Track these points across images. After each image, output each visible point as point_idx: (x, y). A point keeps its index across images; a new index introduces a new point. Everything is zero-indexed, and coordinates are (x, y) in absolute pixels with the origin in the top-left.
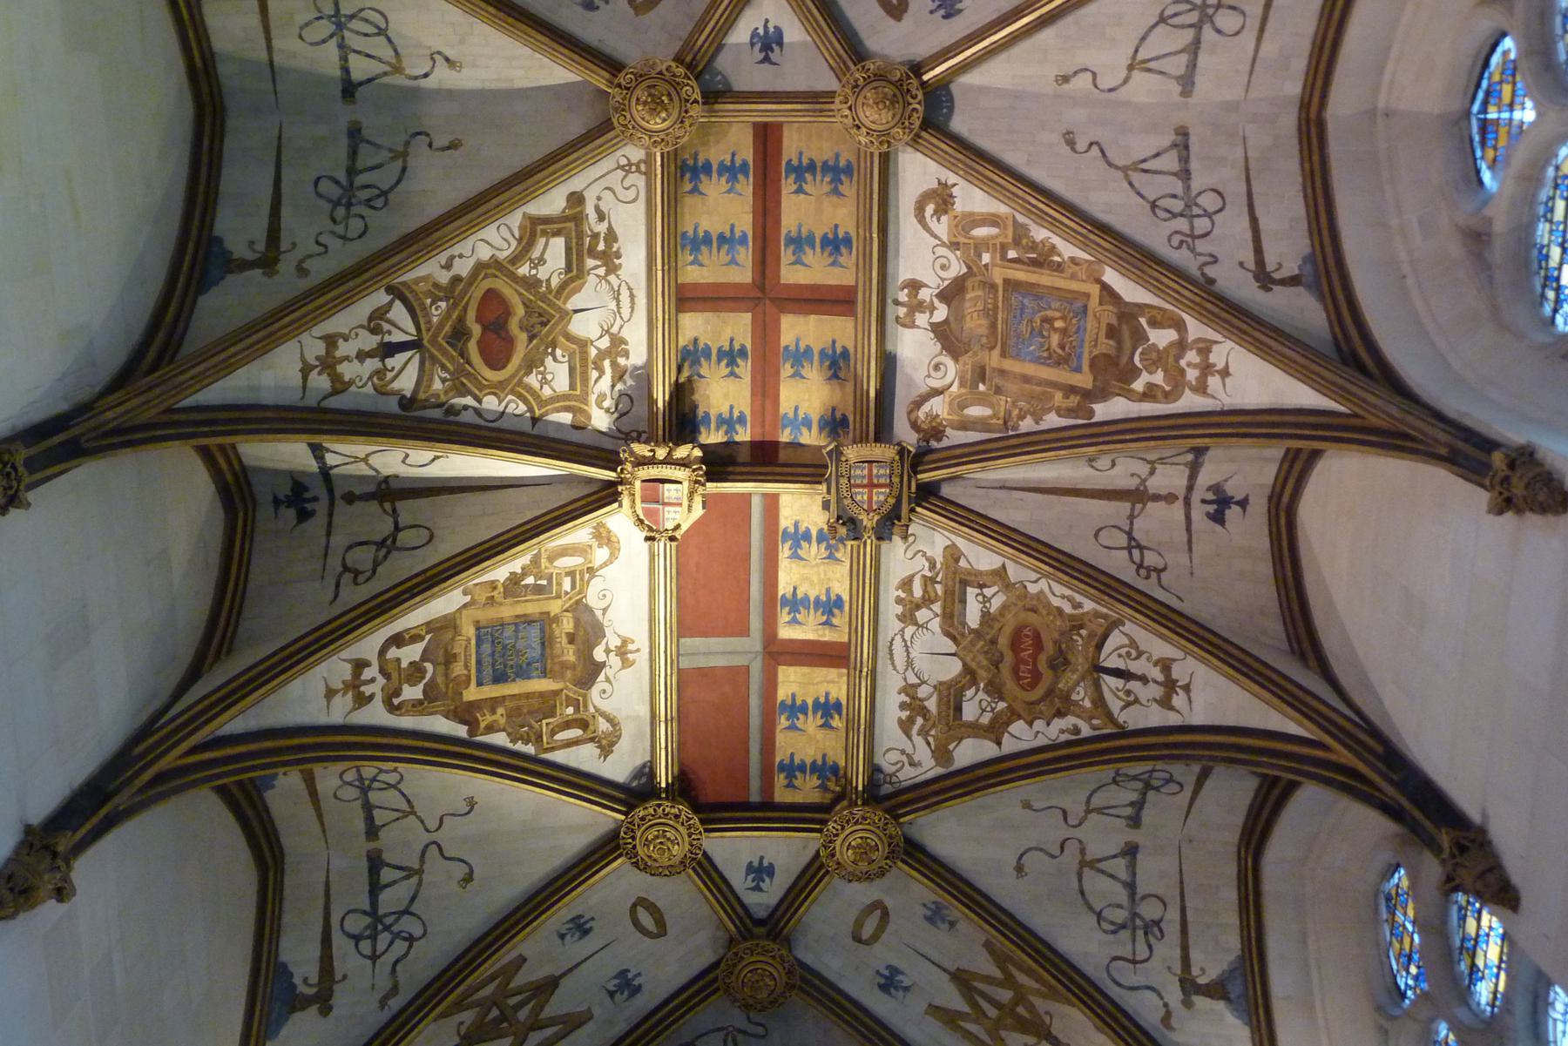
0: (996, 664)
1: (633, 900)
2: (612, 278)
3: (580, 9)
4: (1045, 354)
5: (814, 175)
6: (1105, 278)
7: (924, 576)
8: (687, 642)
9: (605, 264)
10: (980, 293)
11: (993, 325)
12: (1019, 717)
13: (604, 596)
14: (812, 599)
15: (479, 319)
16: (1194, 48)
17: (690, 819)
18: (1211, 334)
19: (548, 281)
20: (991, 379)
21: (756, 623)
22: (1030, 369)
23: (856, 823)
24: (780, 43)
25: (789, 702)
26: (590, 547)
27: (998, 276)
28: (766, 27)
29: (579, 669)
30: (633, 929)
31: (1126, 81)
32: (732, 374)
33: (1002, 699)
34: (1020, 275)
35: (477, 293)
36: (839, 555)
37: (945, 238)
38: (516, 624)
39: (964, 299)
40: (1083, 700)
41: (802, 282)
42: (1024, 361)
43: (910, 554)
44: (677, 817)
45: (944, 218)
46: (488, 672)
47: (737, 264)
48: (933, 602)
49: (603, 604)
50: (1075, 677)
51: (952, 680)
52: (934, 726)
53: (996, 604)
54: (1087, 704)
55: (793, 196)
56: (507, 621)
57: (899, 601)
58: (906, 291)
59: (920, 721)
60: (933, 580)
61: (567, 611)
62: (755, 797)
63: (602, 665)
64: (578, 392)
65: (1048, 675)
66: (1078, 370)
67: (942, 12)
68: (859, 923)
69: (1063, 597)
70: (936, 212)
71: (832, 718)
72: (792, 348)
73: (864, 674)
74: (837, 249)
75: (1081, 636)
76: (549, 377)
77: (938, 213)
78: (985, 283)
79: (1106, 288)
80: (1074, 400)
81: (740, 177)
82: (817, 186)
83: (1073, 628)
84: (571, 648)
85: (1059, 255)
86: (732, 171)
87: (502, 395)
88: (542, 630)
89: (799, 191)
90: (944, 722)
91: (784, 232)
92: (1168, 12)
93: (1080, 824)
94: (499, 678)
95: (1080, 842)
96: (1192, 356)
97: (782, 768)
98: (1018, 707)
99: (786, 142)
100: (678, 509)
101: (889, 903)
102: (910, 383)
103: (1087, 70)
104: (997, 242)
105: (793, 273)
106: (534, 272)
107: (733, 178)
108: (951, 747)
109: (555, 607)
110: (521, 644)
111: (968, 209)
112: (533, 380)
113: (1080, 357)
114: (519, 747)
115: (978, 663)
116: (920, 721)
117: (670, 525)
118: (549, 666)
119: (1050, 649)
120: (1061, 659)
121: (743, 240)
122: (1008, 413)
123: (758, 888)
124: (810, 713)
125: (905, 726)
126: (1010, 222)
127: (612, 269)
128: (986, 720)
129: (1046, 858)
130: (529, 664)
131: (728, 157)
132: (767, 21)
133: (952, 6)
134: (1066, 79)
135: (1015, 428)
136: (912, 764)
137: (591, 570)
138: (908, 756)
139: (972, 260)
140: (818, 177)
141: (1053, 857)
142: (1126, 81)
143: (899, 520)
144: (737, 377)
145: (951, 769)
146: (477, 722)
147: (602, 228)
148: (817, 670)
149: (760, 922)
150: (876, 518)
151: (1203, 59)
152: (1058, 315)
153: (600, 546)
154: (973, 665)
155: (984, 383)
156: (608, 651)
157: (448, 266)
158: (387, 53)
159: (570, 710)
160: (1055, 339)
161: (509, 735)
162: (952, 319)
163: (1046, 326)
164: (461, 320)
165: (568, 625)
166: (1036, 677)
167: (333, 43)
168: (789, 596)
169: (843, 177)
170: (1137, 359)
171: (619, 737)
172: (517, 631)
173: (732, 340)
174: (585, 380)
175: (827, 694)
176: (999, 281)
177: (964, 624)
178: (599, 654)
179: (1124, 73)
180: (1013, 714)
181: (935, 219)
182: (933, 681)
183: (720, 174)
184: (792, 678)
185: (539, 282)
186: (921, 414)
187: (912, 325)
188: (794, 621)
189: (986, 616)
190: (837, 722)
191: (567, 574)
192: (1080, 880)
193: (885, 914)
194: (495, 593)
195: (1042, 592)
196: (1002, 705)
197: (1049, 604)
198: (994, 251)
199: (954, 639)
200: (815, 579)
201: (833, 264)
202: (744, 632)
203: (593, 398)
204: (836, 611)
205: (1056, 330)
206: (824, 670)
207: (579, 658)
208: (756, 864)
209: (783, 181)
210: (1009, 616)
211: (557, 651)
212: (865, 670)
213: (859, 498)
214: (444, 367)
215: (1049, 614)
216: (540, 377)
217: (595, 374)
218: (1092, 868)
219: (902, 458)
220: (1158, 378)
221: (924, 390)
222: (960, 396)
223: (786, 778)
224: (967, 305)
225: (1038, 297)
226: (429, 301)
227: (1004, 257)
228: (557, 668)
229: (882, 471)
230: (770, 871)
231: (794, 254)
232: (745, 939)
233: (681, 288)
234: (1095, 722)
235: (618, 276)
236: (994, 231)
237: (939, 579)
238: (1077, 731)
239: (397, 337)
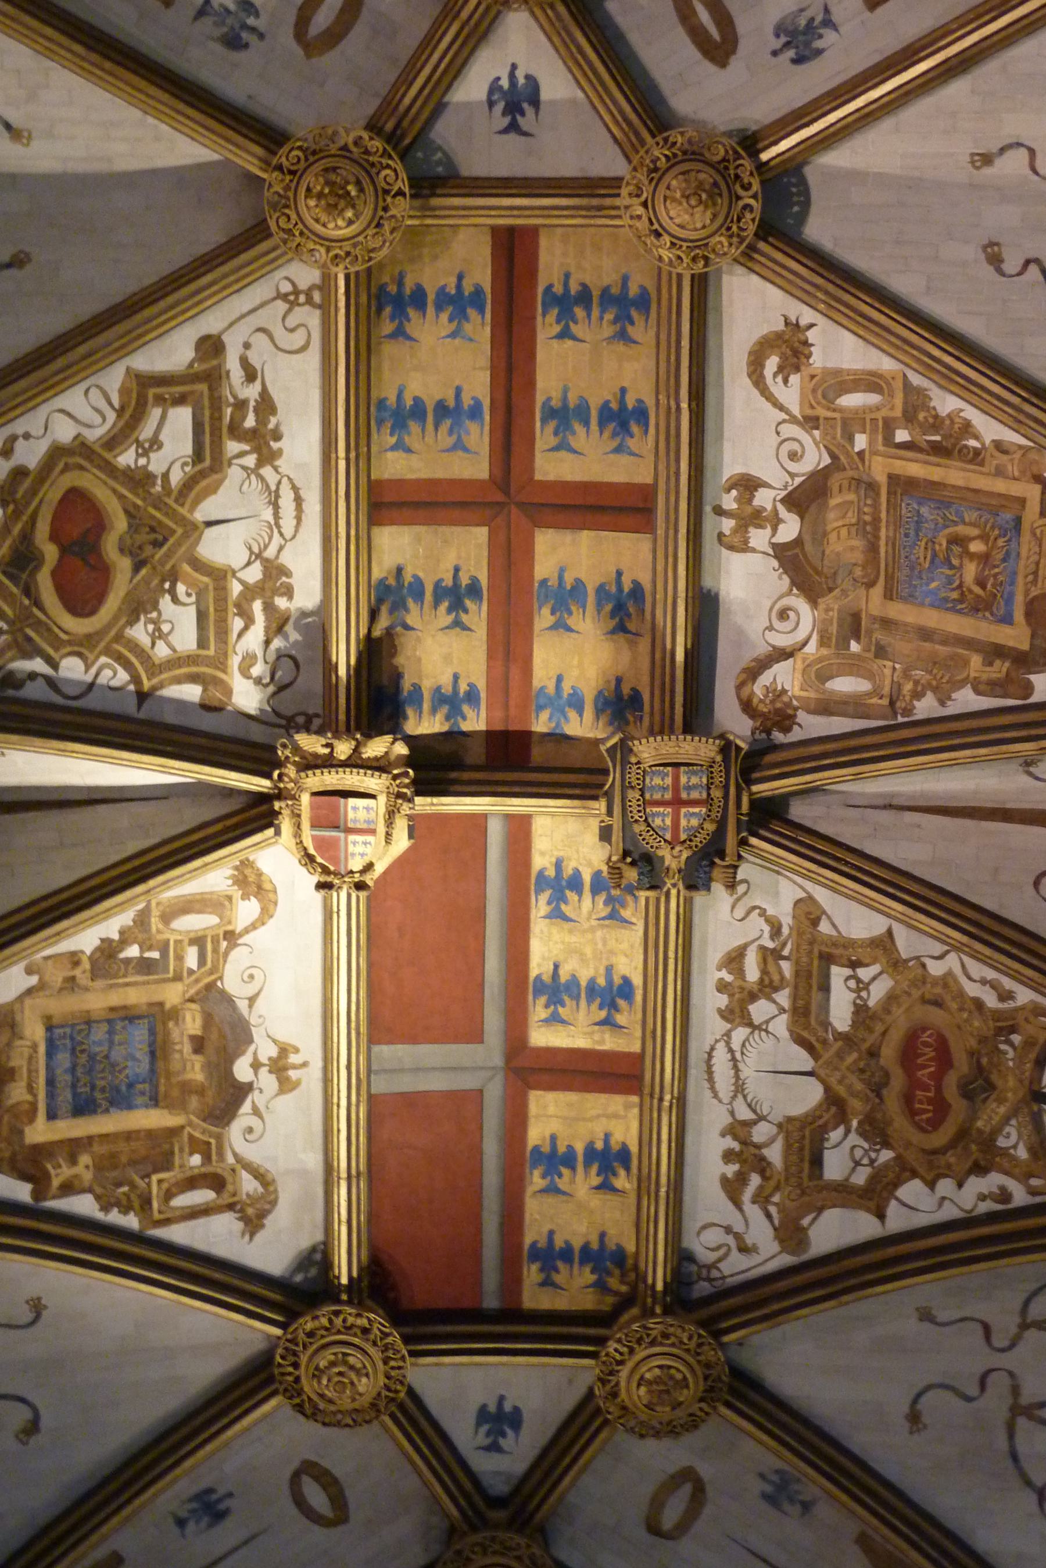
0: (878, 1089)
1: (295, 1464)
2: (267, 471)
3: (219, 48)
4: (955, 595)
5: (588, 309)
7: (763, 948)
8: (384, 1051)
9: (257, 450)
10: (852, 497)
11: (873, 548)
12: (914, 1174)
13: (252, 977)
14: (583, 983)
15: (54, 537)
17: (387, 1335)
19: (166, 476)
20: (870, 632)
21: (493, 1020)
22: (933, 619)
23: (653, 1343)
24: (535, 102)
25: (546, 1149)
26: (230, 898)
27: (879, 470)
28: (512, 76)
29: (210, 1093)
30: (294, 1511)
32: (457, 624)
33: (886, 1144)
34: (915, 469)
35: (53, 494)
36: (626, 913)
37: (796, 411)
38: (109, 1021)
39: (825, 504)
40: (1015, 1147)
41: (569, 478)
42: (922, 604)
43: (739, 913)
44: (365, 1331)
45: (794, 379)
46: (65, 1096)
47: (466, 450)
48: (776, 990)
49: (250, 990)
50: (1002, 1110)
51: (806, 1115)
52: (777, 1188)
53: (877, 993)
54: (1022, 1153)
55: (555, 343)
56: (94, 1016)
57: (722, 987)
58: (734, 492)
59: (755, 1180)
60: (776, 954)
61: (191, 1000)
62: (491, 1302)
63: (245, 1089)
64: (211, 652)
65: (958, 1105)
66: (1007, 619)
67: (791, 53)
68: (657, 1503)
69: (984, 982)
70: (781, 369)
71: (615, 1174)
72: (553, 582)
73: (666, 1104)
74: (624, 427)
75: (1011, 1044)
76: (165, 628)
77: (784, 370)
78: (859, 481)
80: (1000, 668)
81: (472, 313)
83: (999, 1031)
84: (198, 1061)
85: (977, 437)
87: (91, 657)
88: (152, 1032)
89: (564, 334)
90: (793, 1181)
91: (540, 399)
93: (1012, 1345)
94: (83, 1108)
95: (1011, 1374)
97: (535, 1254)
98: (912, 1158)
99: (544, 258)
100: (370, 838)
101: (705, 1470)
102: (740, 638)
103: (1019, 145)
104: (879, 415)
106: (142, 461)
107: (460, 315)
108: (805, 1222)
109: (172, 994)
110: (117, 1054)
111: (830, 365)
112: (140, 633)
113: (1009, 600)
114: (114, 1217)
115: (849, 1088)
116: (755, 1180)
117: (356, 865)
118: (162, 1089)
119: (962, 1065)
120: (980, 1081)
121: (475, 412)
122: (896, 687)
123: (494, 1447)
124: (580, 1168)
125: (733, 1188)
126: (898, 385)
127: (267, 457)
128: (860, 1178)
129: (961, 1403)
130: (130, 1086)
131: (452, 281)
132: (514, 67)
133: (807, 44)
134: (987, 159)
135: (908, 711)
136: (743, 1249)
137: (231, 936)
138: (738, 1236)
139: (839, 446)
140: (595, 312)
141: (969, 1399)
143: (723, 859)
144: (466, 628)
145: (805, 1257)
146: (47, 1177)
147: (251, 393)
148: (591, 1097)
149: (498, 1502)
150: (685, 855)
152: (975, 532)
153: (245, 897)
154: (841, 1090)
155: (858, 640)
156: (256, 1065)
159: (196, 1160)
160: (971, 571)
161: (98, 1198)
162: (807, 538)
163: (956, 549)
164: (27, 537)
165: (192, 1023)
166: (941, 1108)
168: (547, 978)
169: (634, 313)
171: (274, 1203)
172: (111, 1032)
173: (457, 570)
174: (223, 632)
175: (607, 1137)
176: (881, 478)
177: (826, 1024)
178: (242, 1070)
180: (904, 1169)
181: (779, 379)
182: (777, 1117)
183: (439, 308)
184: (552, 1110)
185: (150, 477)
186: (758, 689)
187: (744, 547)
188: (555, 1019)
189: (860, 1010)
190: (622, 1181)
191: (193, 942)
192: (1011, 1435)
193: (699, 1489)
194: (77, 972)
195: (950, 973)
196: (886, 1155)
197: (961, 994)
198: (874, 431)
199: (810, 1048)
200: (588, 951)
201: (618, 450)
202: (475, 1035)
203: (235, 661)
204: (621, 1003)
205: (972, 556)
206: (602, 1098)
207: (210, 1076)
208: (492, 1408)
209: (539, 319)
210: (898, 1012)
211: (175, 1065)
212: (667, 1097)
213: (657, 822)
215: (961, 1009)
216: (150, 627)
217: (238, 623)
218: (1031, 1417)
219: (726, 760)
221: (762, 650)
222: (820, 660)
223: (542, 1270)
224: (831, 515)
225: (944, 504)
227: (889, 440)
228: (175, 1093)
229: (694, 780)
230: (514, 1419)
231: (556, 434)
232: (474, 1529)
233: (375, 487)
234: (1034, 1182)
235: (276, 469)
237: (786, 952)
238: (1004, 1196)
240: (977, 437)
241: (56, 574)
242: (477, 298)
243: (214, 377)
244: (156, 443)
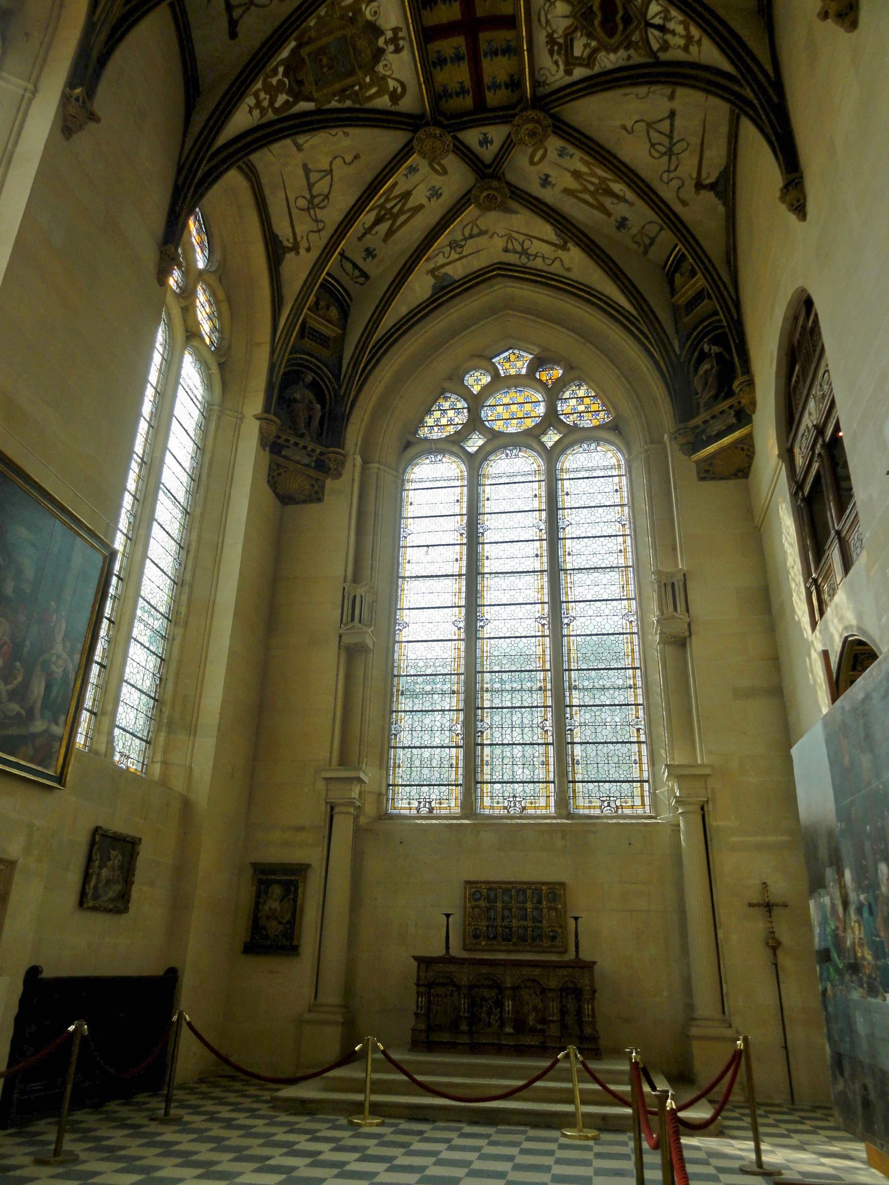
2: (550, 31)
6: (314, 104)
15: (616, 25)
16: (310, 187)
18: (264, 120)
19: (582, 35)
27: (360, 74)
31: (331, 163)
34: (349, 81)
45: (391, 89)
66: (309, 55)
74: (439, 58)
77: (395, 90)
79: (309, 99)
82: (453, 86)
86: (495, 86)
89: (461, 83)
92: (326, 201)
96: (266, 104)
105: (458, 42)
107: (494, 83)
127: (550, 36)
135: (327, 7)
142: (331, 163)
147: (556, 57)
151: (304, 183)
155: (351, 18)
157: (629, 57)
158: (653, 134)
160: (325, 61)
164: (625, 29)
167: (675, 140)
170: (286, 80)
179: (334, 167)
214: (636, 6)
220: (274, 81)
224: (369, 51)
226: (640, 44)
236: (368, 94)
239: (657, 33)
240: (336, 101)
241: (617, 13)
242: (489, 89)
243: (567, 63)
244: (586, 46)
